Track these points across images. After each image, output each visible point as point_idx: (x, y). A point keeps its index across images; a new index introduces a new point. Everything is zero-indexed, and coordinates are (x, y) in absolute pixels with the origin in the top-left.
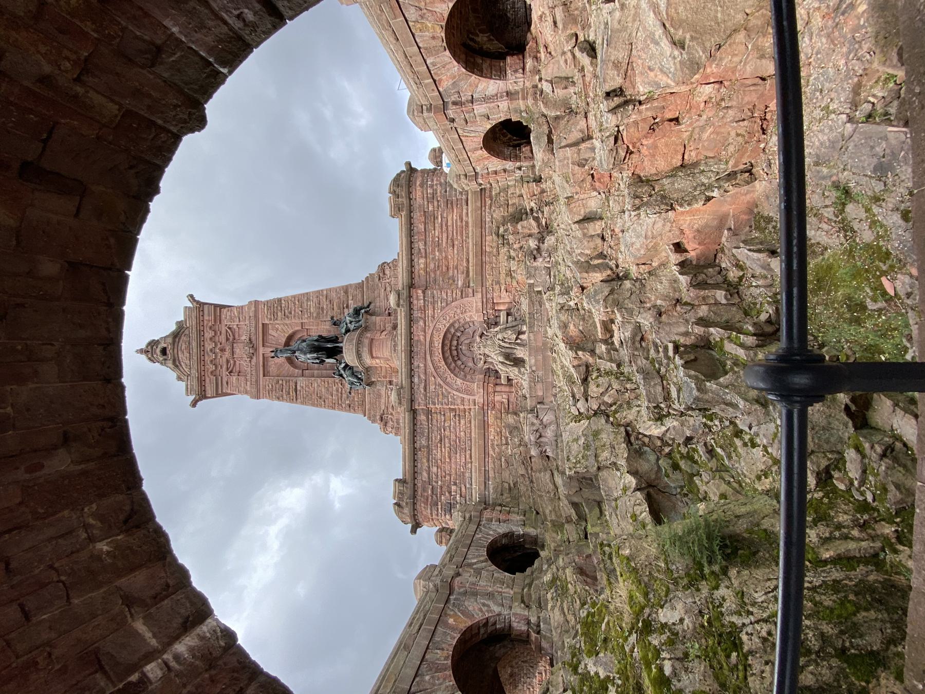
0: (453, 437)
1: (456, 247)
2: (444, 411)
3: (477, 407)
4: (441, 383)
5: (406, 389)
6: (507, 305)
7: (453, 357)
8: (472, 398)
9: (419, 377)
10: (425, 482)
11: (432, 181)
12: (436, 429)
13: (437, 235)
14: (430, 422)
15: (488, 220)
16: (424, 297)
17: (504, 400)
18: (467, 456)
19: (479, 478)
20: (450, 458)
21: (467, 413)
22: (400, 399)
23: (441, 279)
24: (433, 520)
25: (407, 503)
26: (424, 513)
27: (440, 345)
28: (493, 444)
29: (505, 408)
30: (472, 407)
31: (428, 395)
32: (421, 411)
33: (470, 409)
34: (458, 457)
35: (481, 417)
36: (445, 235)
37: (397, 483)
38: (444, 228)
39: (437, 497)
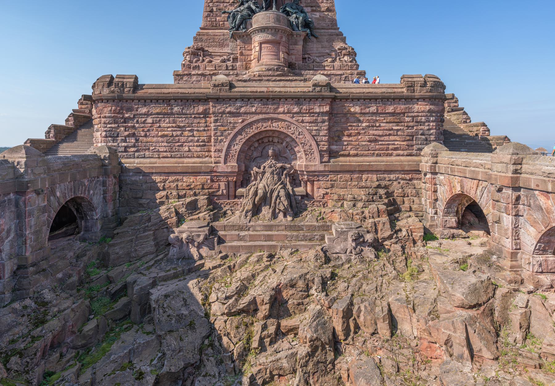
0: (183, 139)
1: (369, 144)
2: (208, 130)
3: (213, 165)
4: (236, 130)
5: (229, 94)
6: (310, 193)
7: (262, 139)
8: (222, 160)
9: (242, 107)
10: (137, 111)
11: (433, 121)
12: (190, 122)
13: (382, 125)
14: (197, 116)
15: (392, 176)
16: (323, 113)
17: (221, 192)
18: (165, 154)
19: (146, 167)
20: (162, 136)
21: (207, 154)
22: (218, 86)
23: (339, 129)
24: (100, 117)
25: (113, 92)
26: (106, 109)
27: (274, 129)
28: (178, 180)
29: (213, 192)
30: (213, 160)
31: (224, 116)
32: (207, 107)
33: (211, 157)
34: (163, 144)
35: (203, 169)
36: (381, 133)
37: (132, 80)
38: (388, 132)
39: (122, 123)
